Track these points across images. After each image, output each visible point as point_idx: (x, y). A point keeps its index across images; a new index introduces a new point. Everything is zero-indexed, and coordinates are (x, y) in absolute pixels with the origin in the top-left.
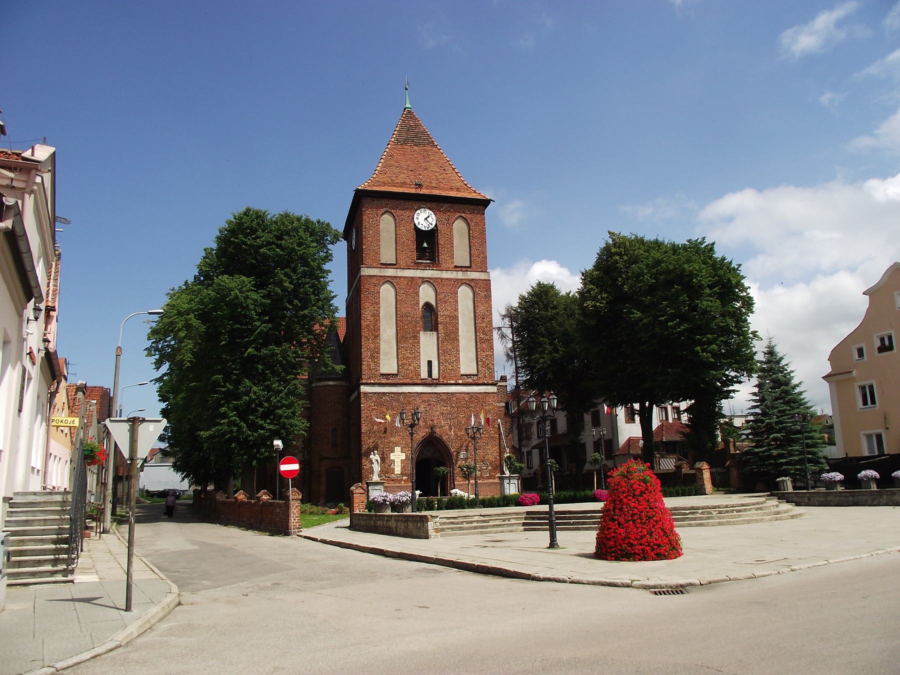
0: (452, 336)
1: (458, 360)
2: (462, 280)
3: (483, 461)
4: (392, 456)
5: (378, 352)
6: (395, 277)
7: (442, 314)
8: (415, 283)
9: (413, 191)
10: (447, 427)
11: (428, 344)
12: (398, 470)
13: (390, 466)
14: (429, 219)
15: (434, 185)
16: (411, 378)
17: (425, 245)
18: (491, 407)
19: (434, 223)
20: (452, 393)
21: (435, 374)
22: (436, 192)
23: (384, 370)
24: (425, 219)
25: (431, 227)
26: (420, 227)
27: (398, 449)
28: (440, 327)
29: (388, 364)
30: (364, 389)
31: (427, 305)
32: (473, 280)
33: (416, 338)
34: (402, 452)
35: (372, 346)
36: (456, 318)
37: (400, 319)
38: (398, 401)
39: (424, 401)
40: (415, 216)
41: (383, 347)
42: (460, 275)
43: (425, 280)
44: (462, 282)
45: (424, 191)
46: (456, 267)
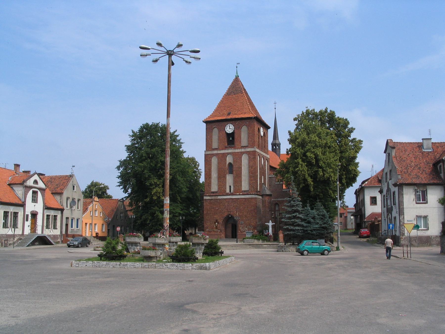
1: (241, 185)
3: (250, 225)
5: (211, 184)
7: (235, 167)
8: (224, 156)
9: (224, 118)
15: (236, 113)
20: (238, 198)
23: (213, 190)
24: (229, 129)
25: (232, 131)
29: (214, 188)
30: (205, 198)
31: (230, 164)
33: (225, 177)
35: (208, 181)
42: (243, 150)
44: (242, 153)
45: (229, 117)
46: (242, 147)
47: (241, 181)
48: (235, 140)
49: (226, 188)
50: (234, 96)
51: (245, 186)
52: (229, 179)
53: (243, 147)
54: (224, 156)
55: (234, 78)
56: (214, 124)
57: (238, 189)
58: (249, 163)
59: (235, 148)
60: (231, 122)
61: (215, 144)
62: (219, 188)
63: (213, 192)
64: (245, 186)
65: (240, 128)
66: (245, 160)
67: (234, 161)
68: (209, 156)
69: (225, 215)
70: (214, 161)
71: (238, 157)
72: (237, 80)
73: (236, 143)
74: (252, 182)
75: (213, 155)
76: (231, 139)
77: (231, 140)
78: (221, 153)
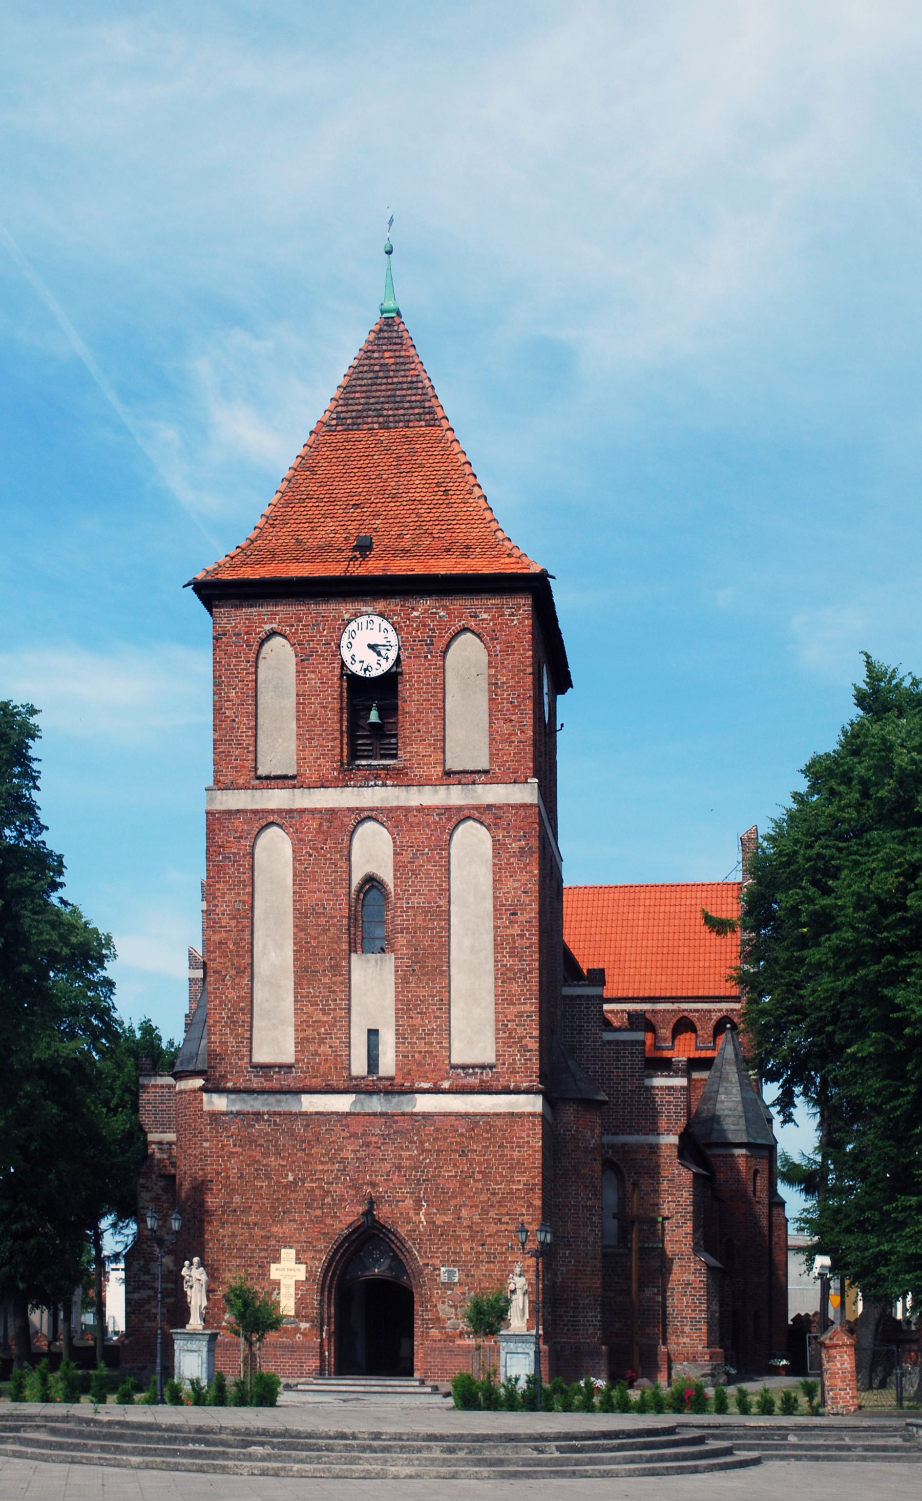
0: (430, 963)
2: (460, 809)
4: (275, 1271)
6: (290, 811)
8: (340, 826)
10: (409, 1202)
11: (373, 987)
15: (406, 543)
19: (393, 655)
21: (388, 1064)
22: (401, 567)
23: (261, 1056)
25: (386, 666)
26: (356, 669)
27: (289, 1255)
28: (401, 940)
31: (372, 882)
32: (489, 807)
34: (298, 1260)
35: (233, 995)
37: (304, 917)
39: (354, 1135)
42: (455, 796)
44: (457, 816)
45: (373, 567)
46: (448, 773)
48: (406, 725)
52: (373, 987)
53: (450, 776)
54: (340, 826)
60: (381, 605)
61: (279, 749)
62: (301, 1043)
63: (266, 1068)
68: (238, 823)
69: (349, 1215)
70: (275, 852)
71: (422, 840)
73: (412, 749)
74: (513, 1010)
75: (265, 820)
78: (313, 811)
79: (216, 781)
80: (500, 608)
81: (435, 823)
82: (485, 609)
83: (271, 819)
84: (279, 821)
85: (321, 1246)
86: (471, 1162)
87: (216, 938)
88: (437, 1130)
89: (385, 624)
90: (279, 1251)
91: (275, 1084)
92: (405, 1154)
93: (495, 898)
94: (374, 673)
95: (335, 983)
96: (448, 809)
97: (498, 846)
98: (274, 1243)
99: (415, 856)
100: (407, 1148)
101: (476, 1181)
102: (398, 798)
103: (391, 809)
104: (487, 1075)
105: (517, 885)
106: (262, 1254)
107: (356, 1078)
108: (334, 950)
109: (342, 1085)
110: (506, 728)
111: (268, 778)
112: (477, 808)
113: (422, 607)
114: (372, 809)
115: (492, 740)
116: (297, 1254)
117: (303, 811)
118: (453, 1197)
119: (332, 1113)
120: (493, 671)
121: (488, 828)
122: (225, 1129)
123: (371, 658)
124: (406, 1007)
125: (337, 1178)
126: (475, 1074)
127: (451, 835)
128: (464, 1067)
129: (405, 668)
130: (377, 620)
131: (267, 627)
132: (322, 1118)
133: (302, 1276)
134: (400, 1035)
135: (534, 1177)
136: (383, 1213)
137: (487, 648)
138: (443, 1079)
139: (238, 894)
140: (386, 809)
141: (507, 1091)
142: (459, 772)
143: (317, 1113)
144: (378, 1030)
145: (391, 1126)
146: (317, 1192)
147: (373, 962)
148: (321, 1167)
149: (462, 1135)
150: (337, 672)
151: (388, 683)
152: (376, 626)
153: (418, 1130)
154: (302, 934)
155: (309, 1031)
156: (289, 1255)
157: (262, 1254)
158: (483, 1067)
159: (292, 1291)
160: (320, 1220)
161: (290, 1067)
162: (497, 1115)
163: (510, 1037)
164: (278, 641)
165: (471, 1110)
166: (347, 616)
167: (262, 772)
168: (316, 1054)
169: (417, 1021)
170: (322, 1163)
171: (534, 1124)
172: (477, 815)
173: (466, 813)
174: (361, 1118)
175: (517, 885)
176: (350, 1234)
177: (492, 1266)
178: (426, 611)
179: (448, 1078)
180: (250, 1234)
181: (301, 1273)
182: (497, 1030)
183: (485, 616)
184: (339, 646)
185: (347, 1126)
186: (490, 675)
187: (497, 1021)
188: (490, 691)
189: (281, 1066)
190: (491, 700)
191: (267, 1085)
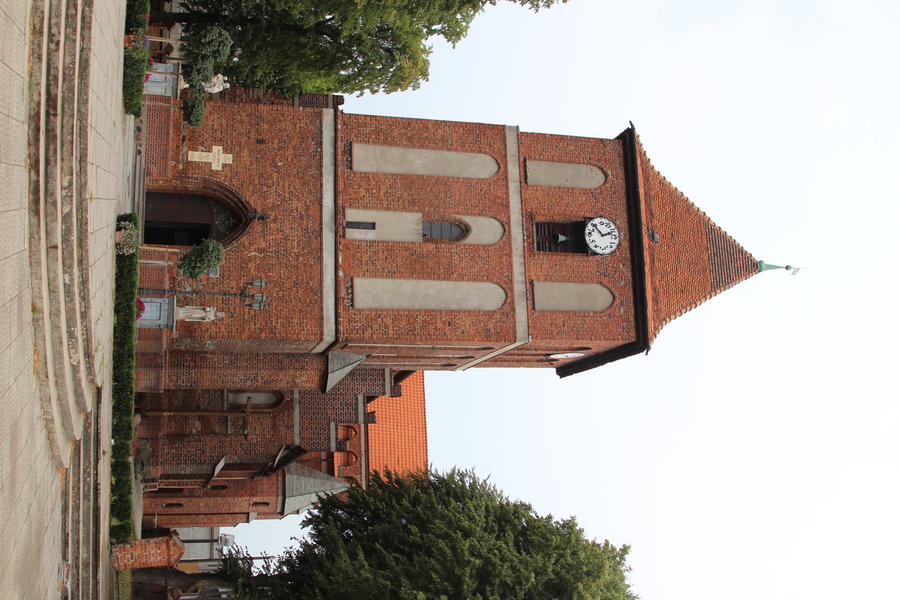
1: (376, 274)
2: (512, 290)
4: (217, 149)
5: (386, 142)
6: (506, 179)
7: (454, 252)
10: (263, 245)
11: (401, 226)
12: (195, 156)
13: (203, 144)
14: (604, 230)
16: (345, 191)
17: (562, 238)
18: (297, 328)
19: (598, 250)
20: (320, 259)
23: (358, 150)
24: (603, 238)
25: (592, 246)
26: (589, 227)
27: (229, 159)
28: (431, 247)
31: (465, 230)
32: (514, 309)
36: (448, 277)
38: (310, 166)
39: (307, 209)
40: (605, 221)
41: (395, 152)
42: (519, 287)
43: (506, 226)
44: (508, 291)
46: (532, 283)
47: (392, 275)
48: (559, 258)
49: (365, 207)
50: (705, 256)
51: (373, 292)
52: (401, 226)
55: (757, 257)
56: (621, 174)
57: (355, 260)
58: (468, 313)
59: (529, 252)
60: (626, 244)
62: (366, 176)
63: (349, 152)
64: (373, 292)
65: (602, 278)
66: (483, 296)
67: (476, 247)
71: (492, 265)
72: (751, 266)
73: (545, 260)
76: (562, 238)
77: (561, 237)
78: (507, 193)
79: (522, 133)
80: (627, 320)
81: (503, 273)
82: (627, 310)
83: (502, 166)
84: (501, 171)
85: (235, 182)
86: (290, 289)
87: (430, 126)
88: (311, 266)
89: (614, 246)
90: (231, 153)
91: (340, 157)
92: (295, 243)
93: (459, 311)
94: (587, 238)
95: (404, 201)
96: (511, 282)
97: (490, 314)
98: (237, 149)
99: (483, 259)
100: (299, 245)
101: (277, 292)
102: (517, 249)
103: (510, 245)
104: (347, 303)
105: (467, 326)
106: (229, 141)
107: (344, 212)
108: (424, 202)
109: (340, 202)
110: (559, 322)
111: (525, 166)
112: (513, 302)
113: (626, 271)
114: (509, 232)
115: (553, 312)
116: (229, 165)
117: (507, 187)
118: (267, 276)
119: (322, 195)
120: (591, 314)
121: (501, 308)
122: (311, 122)
123: (607, 240)
124: (390, 248)
125: (279, 195)
126: (348, 294)
127: (496, 283)
128: (352, 286)
129: (591, 258)
130: (617, 242)
131: (609, 173)
132: (319, 187)
133: (215, 167)
134: (372, 242)
135: (280, 333)
136: (256, 226)
137: (604, 311)
138: (344, 272)
139: (457, 142)
140: (510, 242)
141: (337, 315)
142: (533, 291)
143: (322, 184)
144: (374, 228)
145: (313, 234)
146: (270, 181)
147: (417, 228)
148: (287, 184)
149: (308, 283)
150: (587, 215)
151: (579, 246)
152: (613, 241)
153: (311, 253)
154: (434, 181)
155: (373, 183)
156: (229, 159)
157: (229, 141)
158: (352, 300)
159: (204, 160)
160: (251, 182)
161: (351, 168)
162: (322, 309)
163: (372, 319)
164: (601, 178)
165: (325, 290)
166: (618, 222)
167: (528, 163)
168: (359, 186)
169: (381, 256)
170: (289, 186)
171: (315, 334)
172: (509, 301)
173: (510, 294)
174: (318, 214)
175: (467, 326)
176: (242, 203)
177: (220, 302)
178: (623, 273)
179: (345, 276)
180: (243, 134)
181: (216, 167)
182: (376, 310)
183: (622, 311)
184: (601, 217)
185: (313, 204)
186: (589, 312)
187: (382, 310)
188: (580, 312)
189: (351, 162)
190: (575, 313)
191: (339, 151)
